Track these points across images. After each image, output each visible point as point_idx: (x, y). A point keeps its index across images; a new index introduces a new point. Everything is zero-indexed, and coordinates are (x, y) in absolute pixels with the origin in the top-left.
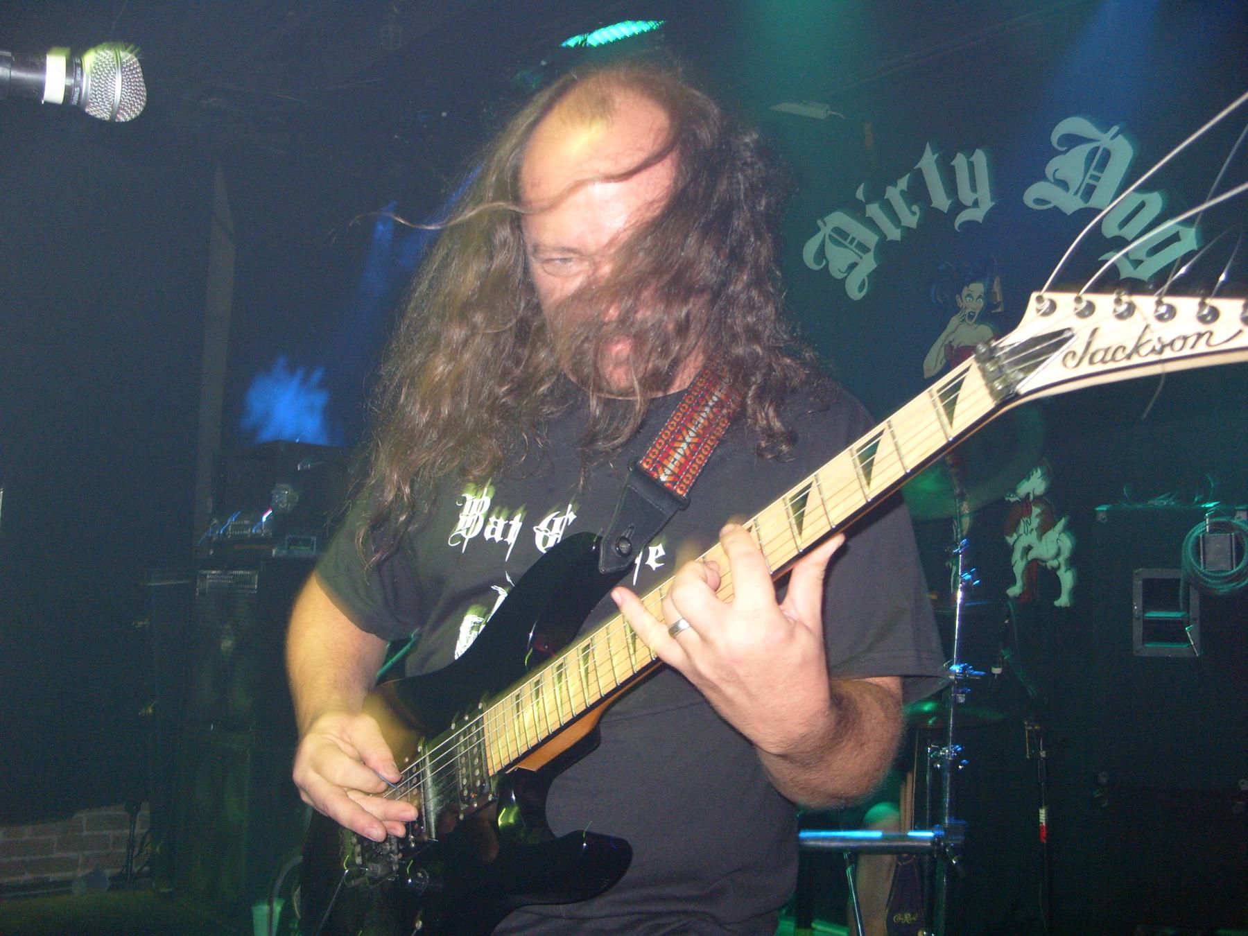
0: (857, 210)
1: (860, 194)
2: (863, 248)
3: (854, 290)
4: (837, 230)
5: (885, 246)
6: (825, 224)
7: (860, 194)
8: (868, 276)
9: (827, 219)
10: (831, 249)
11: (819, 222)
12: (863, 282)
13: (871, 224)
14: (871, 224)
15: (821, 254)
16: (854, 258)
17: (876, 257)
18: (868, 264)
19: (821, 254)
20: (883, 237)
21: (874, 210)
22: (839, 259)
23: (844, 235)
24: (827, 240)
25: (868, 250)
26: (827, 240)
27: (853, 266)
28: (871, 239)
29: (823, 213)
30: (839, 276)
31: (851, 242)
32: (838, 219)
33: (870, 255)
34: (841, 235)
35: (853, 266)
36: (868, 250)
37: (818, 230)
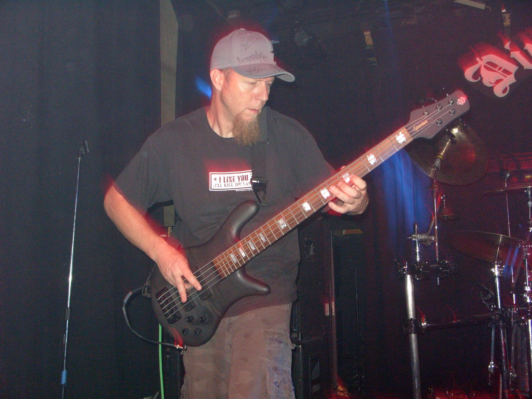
0: (506, 55)
2: (507, 72)
3: (499, 92)
4: (488, 63)
5: (521, 72)
6: (482, 60)
7: (507, 46)
8: (510, 86)
10: (484, 73)
11: (478, 59)
13: (515, 62)
14: (515, 62)
15: (477, 74)
16: (501, 77)
18: (511, 80)
19: (477, 74)
21: (516, 55)
22: (488, 78)
23: (495, 66)
24: (483, 68)
27: (498, 81)
28: (513, 68)
30: (489, 85)
35: (498, 81)
37: (477, 62)
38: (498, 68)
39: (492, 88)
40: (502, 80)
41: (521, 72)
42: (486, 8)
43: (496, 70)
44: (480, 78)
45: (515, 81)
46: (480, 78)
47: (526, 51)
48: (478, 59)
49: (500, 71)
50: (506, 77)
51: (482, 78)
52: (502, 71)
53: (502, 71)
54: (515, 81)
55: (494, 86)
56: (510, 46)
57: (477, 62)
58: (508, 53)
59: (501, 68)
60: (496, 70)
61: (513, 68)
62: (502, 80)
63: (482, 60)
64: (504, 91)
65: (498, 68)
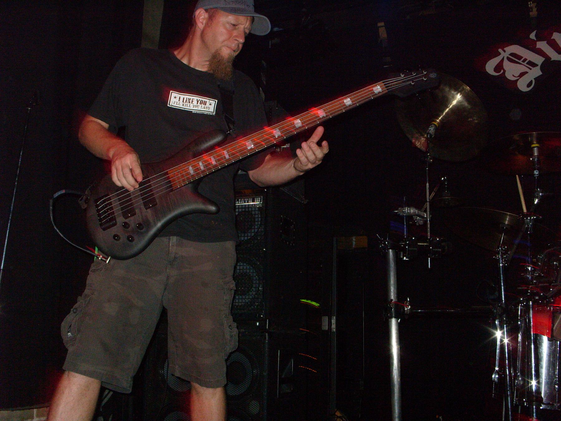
1: (533, 36)
2: (532, 64)
3: (522, 86)
4: (512, 54)
5: (548, 64)
6: (505, 51)
7: (533, 36)
9: (505, 49)
10: (507, 65)
11: (500, 50)
12: (532, 81)
13: (540, 52)
14: (540, 52)
15: (499, 67)
17: (542, 69)
18: (536, 72)
19: (499, 67)
20: (547, 58)
21: (542, 45)
22: (512, 71)
23: (519, 57)
24: (505, 59)
25: (536, 65)
26: (505, 59)
27: (522, 74)
28: (539, 60)
30: (515, 79)
31: (524, 61)
33: (538, 68)
34: (515, 58)
35: (522, 74)
36: (536, 65)
37: (500, 54)
38: (522, 60)
40: (527, 73)
41: (548, 64)
43: (520, 62)
44: (502, 71)
45: (541, 73)
47: (554, 40)
48: (500, 50)
49: (525, 64)
50: (531, 69)
51: (505, 71)
52: (527, 63)
53: (527, 63)
54: (541, 73)
55: (518, 80)
56: (536, 36)
57: (500, 54)
58: (534, 42)
59: (525, 60)
61: (539, 60)
62: (527, 73)
63: (505, 51)
64: (529, 85)
65: (522, 60)
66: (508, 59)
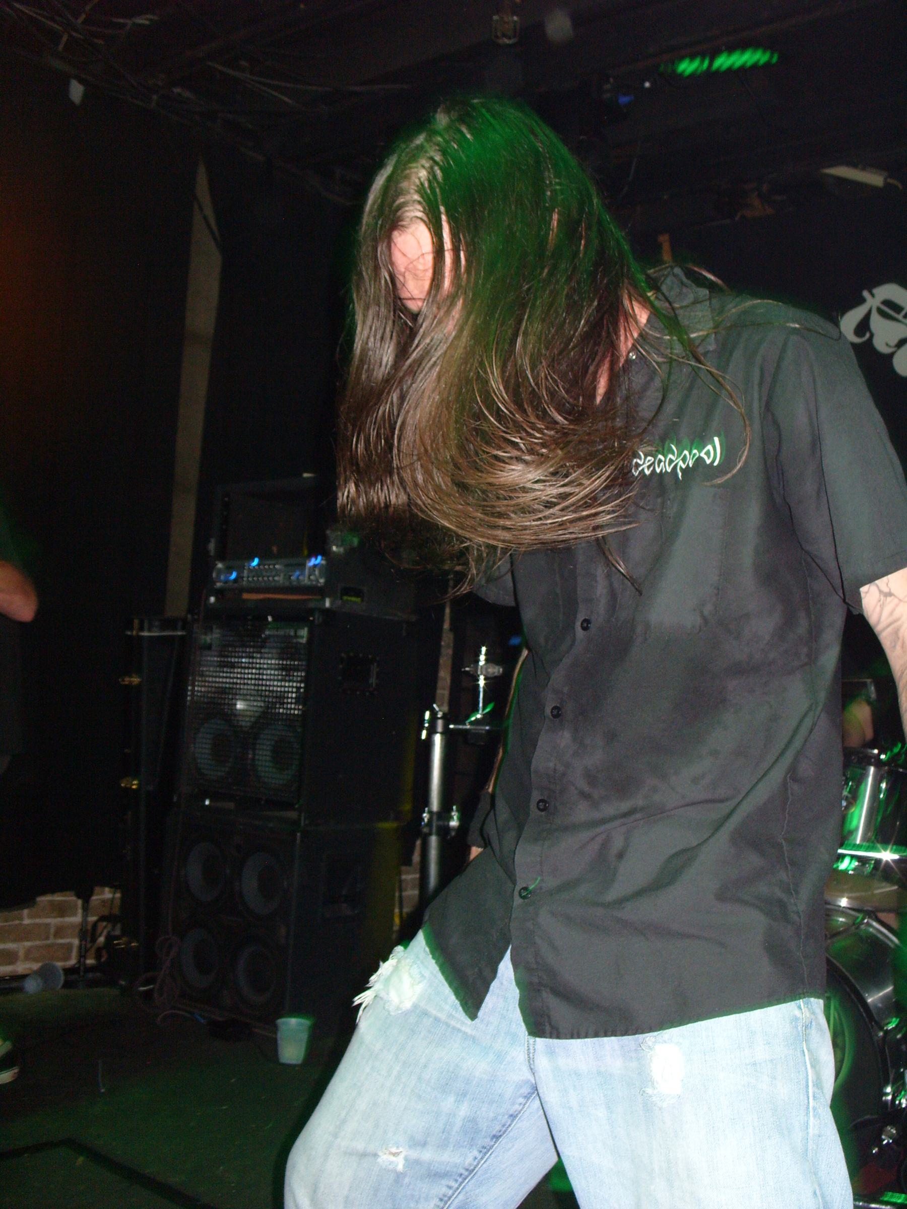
4: (888, 303)
6: (873, 295)
9: (875, 291)
10: (876, 321)
11: (866, 294)
15: (863, 327)
19: (863, 327)
24: (874, 312)
26: (874, 312)
29: (873, 283)
32: (889, 291)
37: (863, 301)
39: (892, 355)
42: (887, 185)
43: (900, 317)
44: (868, 335)
46: (868, 335)
48: (866, 294)
51: (872, 335)
60: (900, 317)
63: (873, 295)
66: (881, 312)
